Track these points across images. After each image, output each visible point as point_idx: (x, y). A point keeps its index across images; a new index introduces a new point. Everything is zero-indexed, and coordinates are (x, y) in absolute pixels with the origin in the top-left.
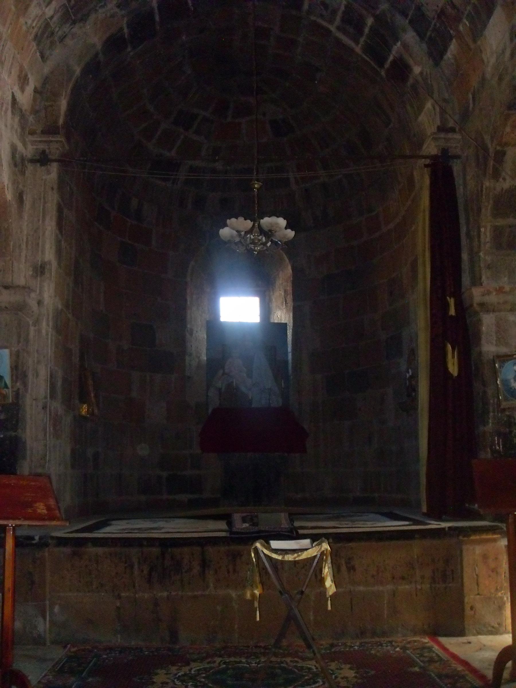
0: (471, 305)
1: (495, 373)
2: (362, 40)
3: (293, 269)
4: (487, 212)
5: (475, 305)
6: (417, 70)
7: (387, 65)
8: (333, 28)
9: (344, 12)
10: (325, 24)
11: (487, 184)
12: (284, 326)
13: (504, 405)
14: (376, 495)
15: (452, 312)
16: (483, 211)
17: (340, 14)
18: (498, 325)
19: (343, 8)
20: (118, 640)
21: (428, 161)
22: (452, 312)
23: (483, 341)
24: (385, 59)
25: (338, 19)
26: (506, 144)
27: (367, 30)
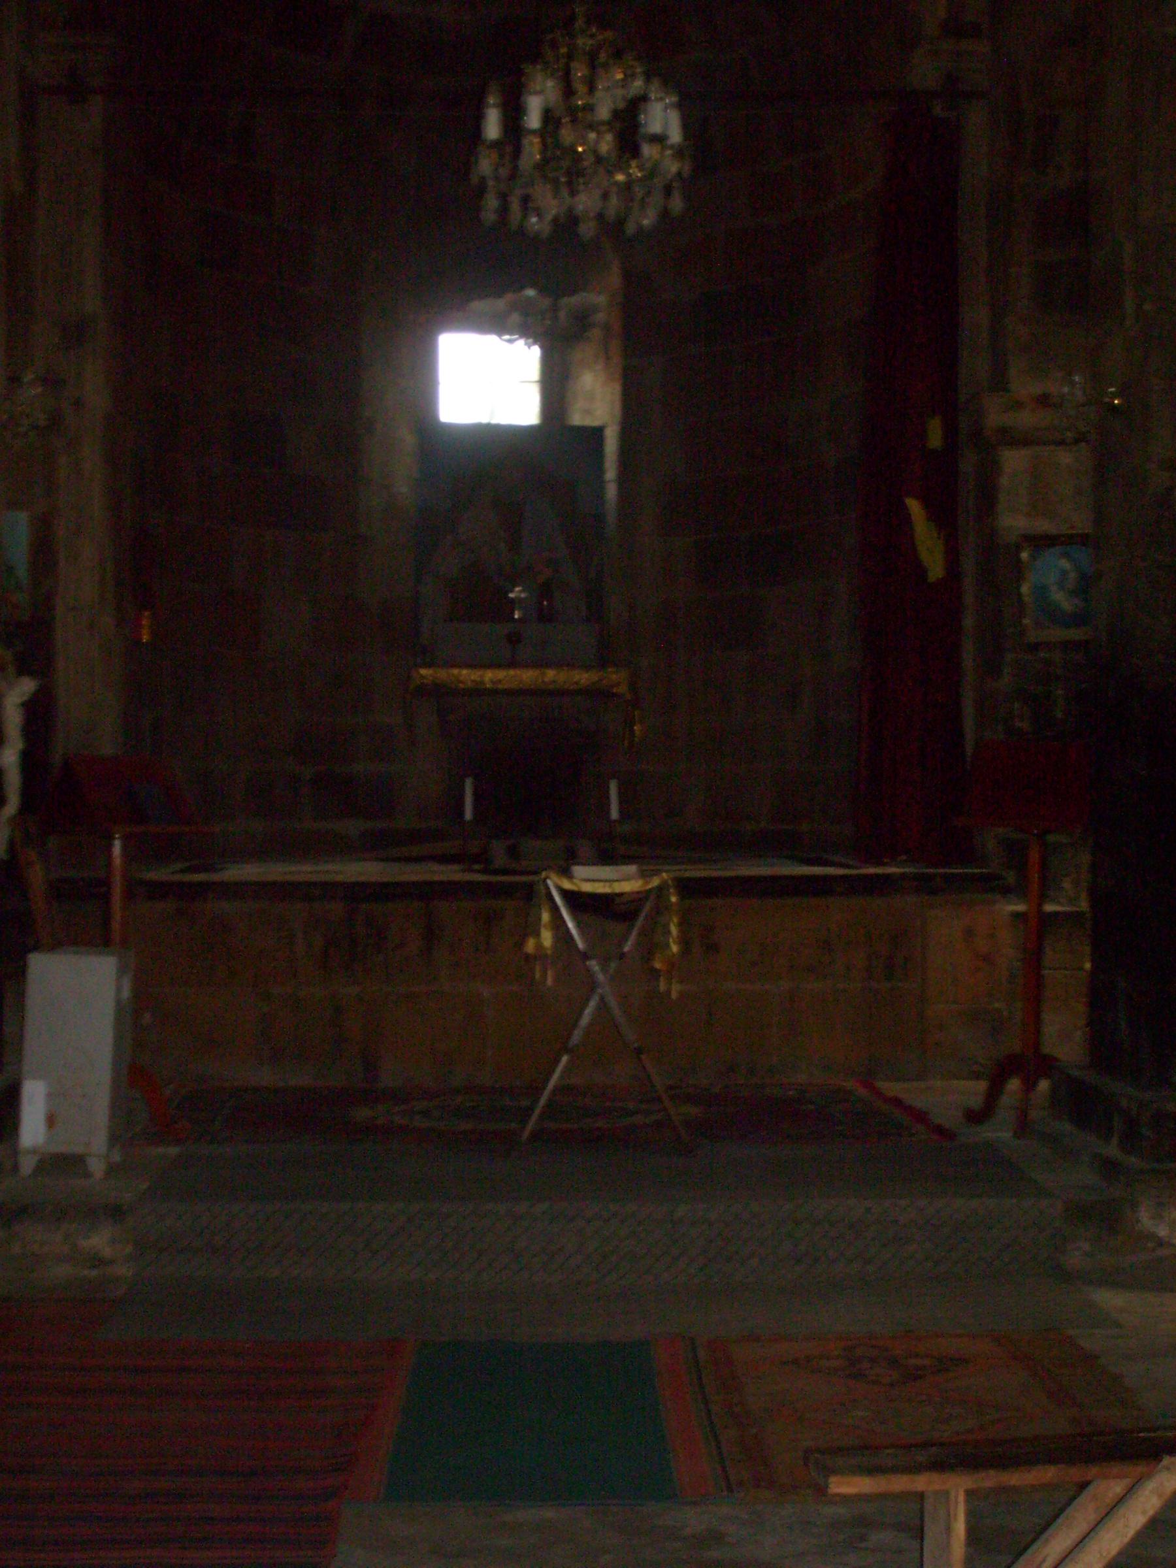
1: (1018, 571)
3: (627, 276)
12: (596, 435)
13: (1032, 636)
14: (805, 827)
20: (266, 1076)
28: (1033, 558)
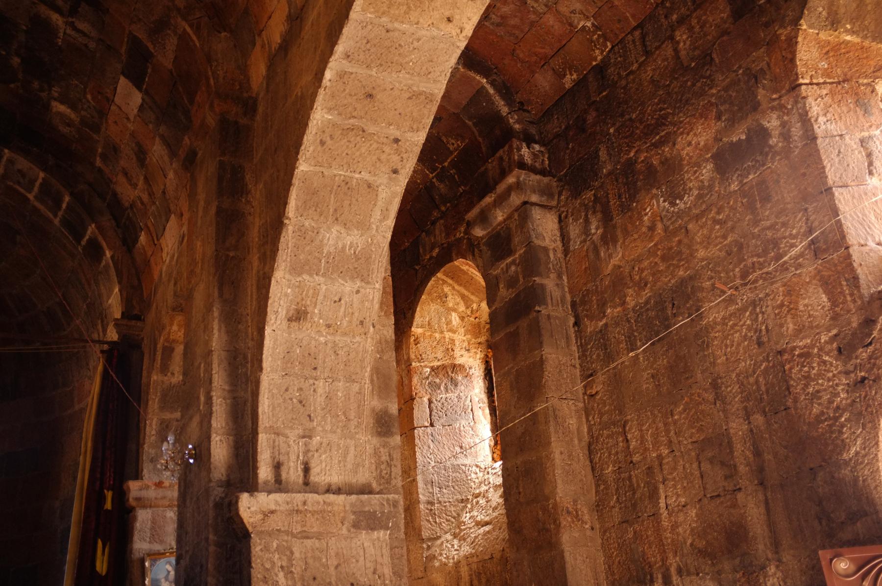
0: (128, 500)
1: (143, 573)
2: (60, 214)
4: (154, 403)
5: (131, 500)
6: (108, 254)
7: (83, 242)
8: (31, 196)
9: (41, 184)
10: (22, 191)
11: (154, 377)
15: (108, 506)
16: (150, 403)
17: (37, 184)
18: (154, 522)
19: (40, 181)
21: (106, 347)
22: (108, 506)
23: (136, 538)
24: (83, 236)
25: (36, 189)
26: (174, 341)
27: (64, 206)
28: (151, 565)
